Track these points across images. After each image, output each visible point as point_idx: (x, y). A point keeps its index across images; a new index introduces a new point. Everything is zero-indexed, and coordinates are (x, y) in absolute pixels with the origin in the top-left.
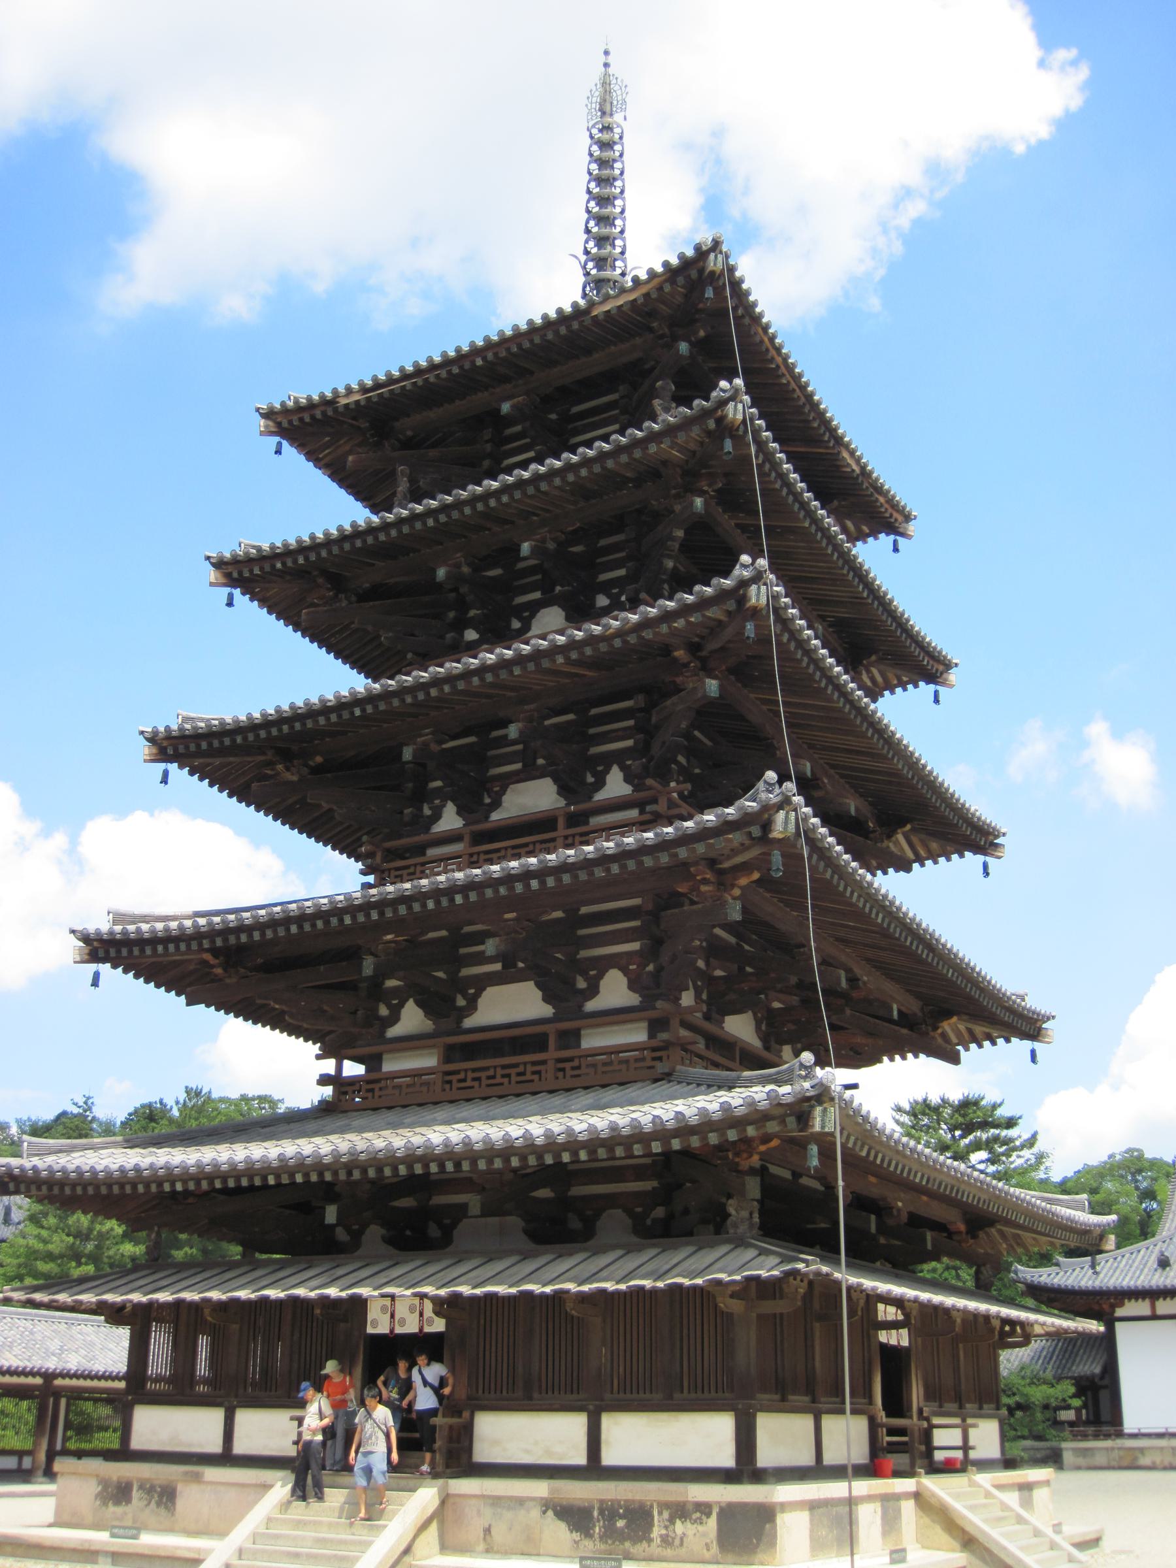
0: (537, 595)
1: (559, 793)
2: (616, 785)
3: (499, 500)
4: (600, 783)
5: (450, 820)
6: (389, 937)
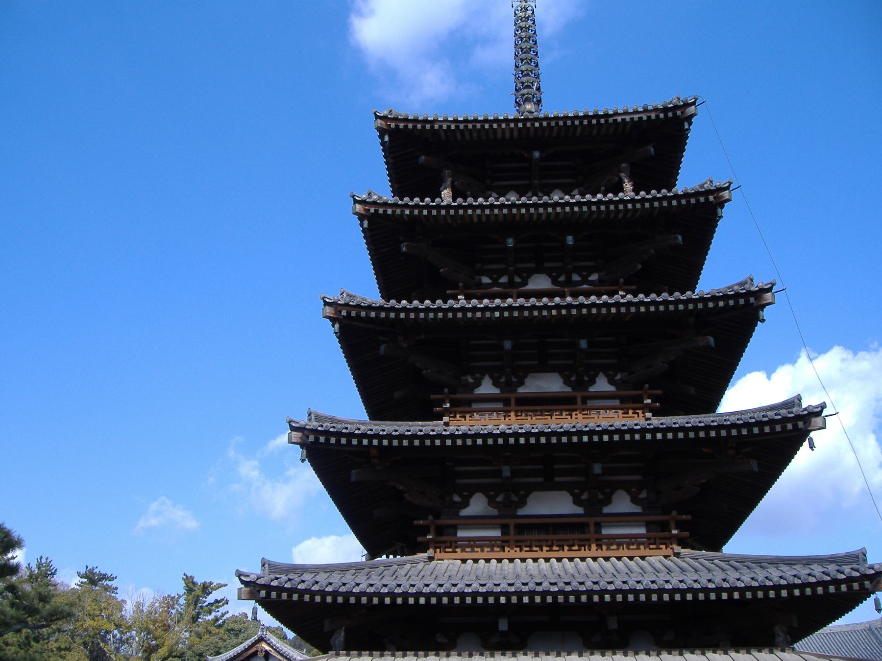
0: (532, 265)
1: (564, 383)
2: (602, 385)
3: (572, 209)
4: (592, 382)
5: (487, 388)
6: (508, 454)
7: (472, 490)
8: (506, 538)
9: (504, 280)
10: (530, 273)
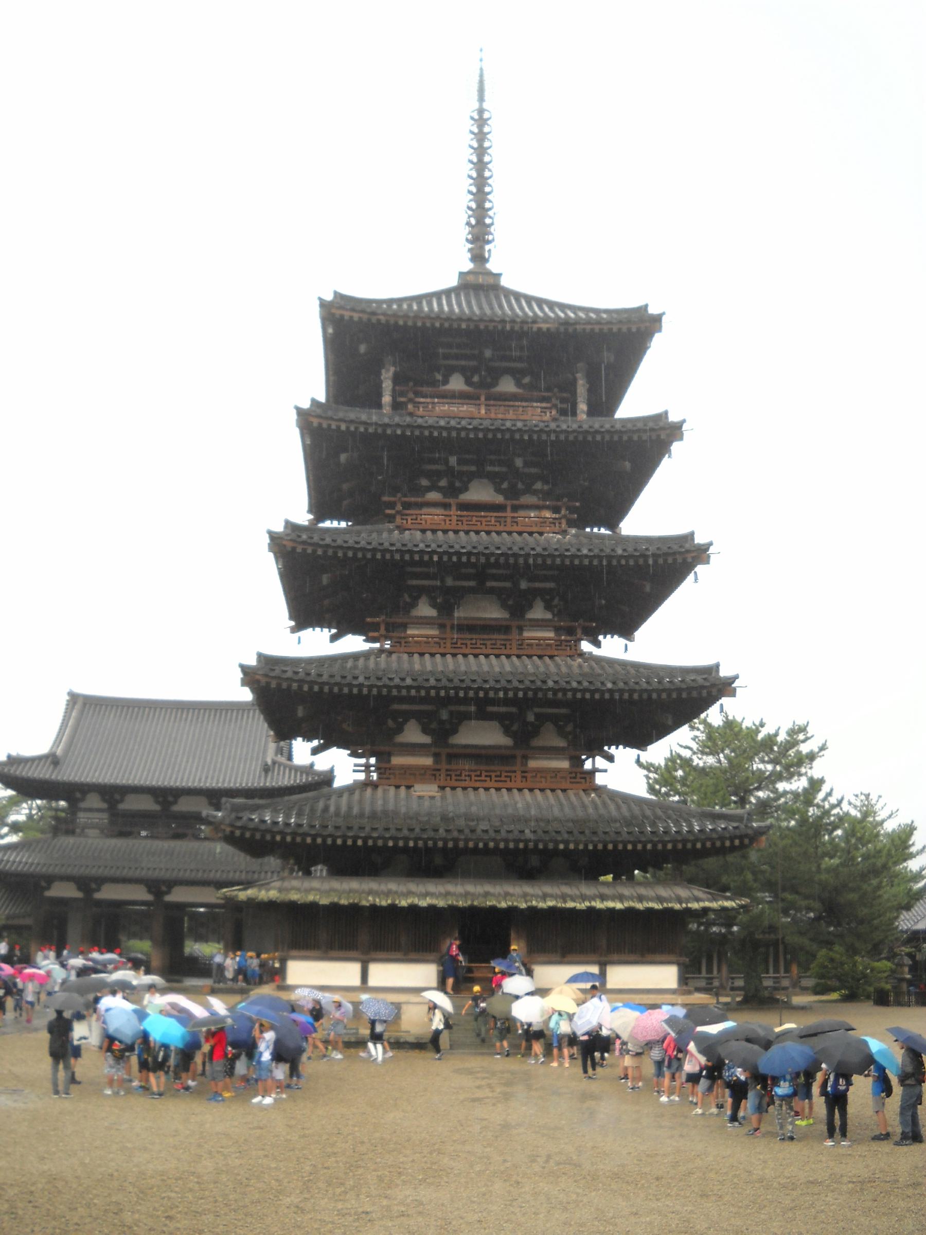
0: (473, 468)
7: (408, 716)
8: (438, 767)
9: (443, 483)
10: (472, 476)
